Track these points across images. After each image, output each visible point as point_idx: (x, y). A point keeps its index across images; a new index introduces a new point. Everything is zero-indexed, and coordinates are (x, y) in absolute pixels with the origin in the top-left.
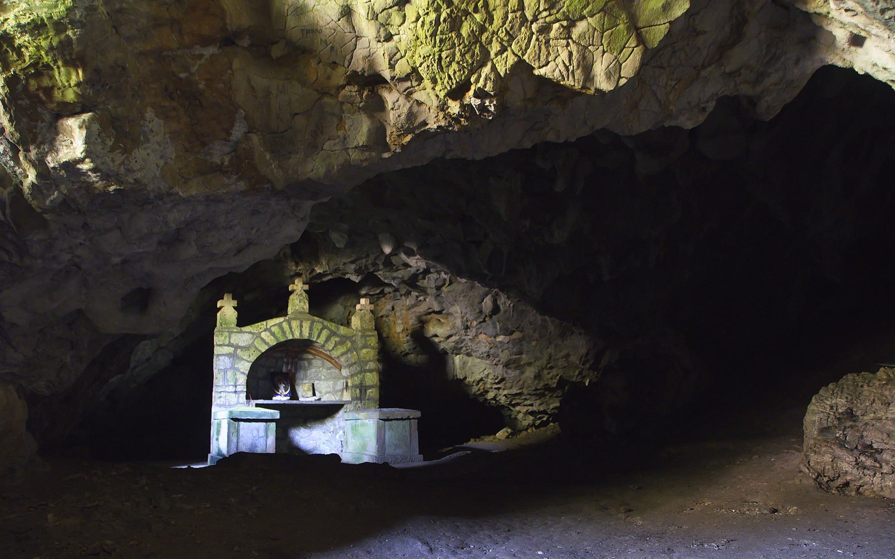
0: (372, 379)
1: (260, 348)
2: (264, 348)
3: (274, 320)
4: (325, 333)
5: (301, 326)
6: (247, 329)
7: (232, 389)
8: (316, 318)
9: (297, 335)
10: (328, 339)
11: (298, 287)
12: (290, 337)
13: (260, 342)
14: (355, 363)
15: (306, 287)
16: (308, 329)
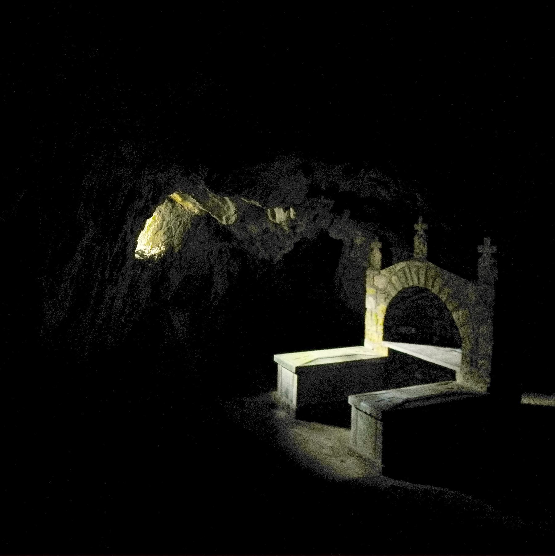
0: (486, 348)
1: (392, 293)
2: (393, 293)
3: (399, 264)
4: (438, 283)
5: (418, 272)
6: (384, 272)
7: (374, 328)
8: (430, 263)
9: (416, 283)
10: (441, 289)
11: (420, 227)
12: (411, 284)
13: (392, 286)
14: (466, 324)
15: (425, 226)
16: (424, 276)
